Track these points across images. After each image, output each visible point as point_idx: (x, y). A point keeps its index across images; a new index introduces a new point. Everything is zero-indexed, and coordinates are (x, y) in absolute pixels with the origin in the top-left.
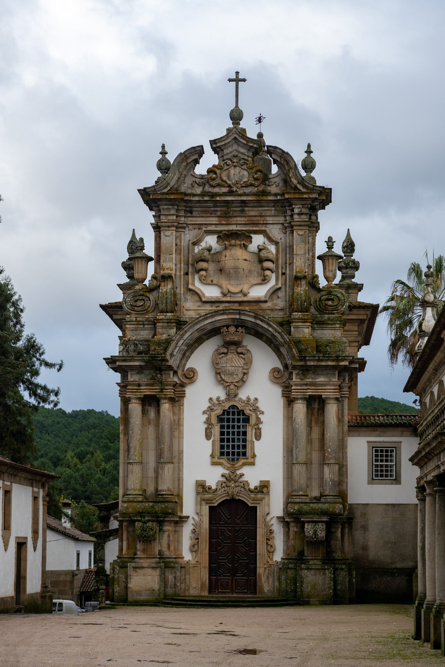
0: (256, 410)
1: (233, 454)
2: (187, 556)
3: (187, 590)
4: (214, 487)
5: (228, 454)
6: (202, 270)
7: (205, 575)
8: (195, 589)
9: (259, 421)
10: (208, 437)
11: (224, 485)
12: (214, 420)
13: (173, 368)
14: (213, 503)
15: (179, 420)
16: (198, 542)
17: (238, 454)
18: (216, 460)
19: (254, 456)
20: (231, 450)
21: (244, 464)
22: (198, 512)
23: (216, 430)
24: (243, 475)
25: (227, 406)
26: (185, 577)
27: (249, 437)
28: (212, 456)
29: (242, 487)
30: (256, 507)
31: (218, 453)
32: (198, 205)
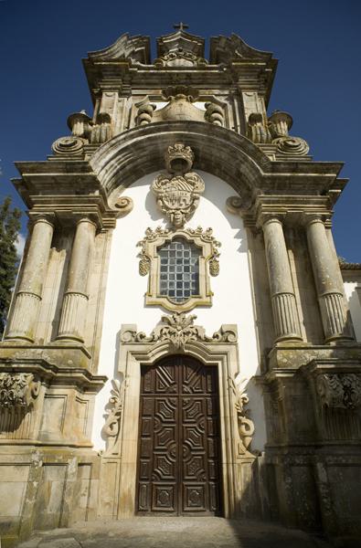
0: (210, 240)
1: (179, 293)
2: (98, 444)
3: (92, 509)
4: (148, 336)
5: (172, 293)
6: (144, 119)
7: (129, 481)
8: (107, 507)
9: (214, 255)
10: (142, 272)
11: (165, 330)
12: (152, 251)
13: (98, 182)
14: (148, 359)
15: (105, 251)
16: (119, 420)
17: (187, 293)
18: (154, 299)
19: (210, 295)
20: (175, 288)
21: (198, 306)
22: (122, 369)
23: (156, 263)
24: (195, 318)
25: (171, 236)
26: (90, 483)
27: (202, 272)
28: (148, 294)
29: (193, 334)
30: (216, 367)
31: (156, 289)
32: (143, 81)
